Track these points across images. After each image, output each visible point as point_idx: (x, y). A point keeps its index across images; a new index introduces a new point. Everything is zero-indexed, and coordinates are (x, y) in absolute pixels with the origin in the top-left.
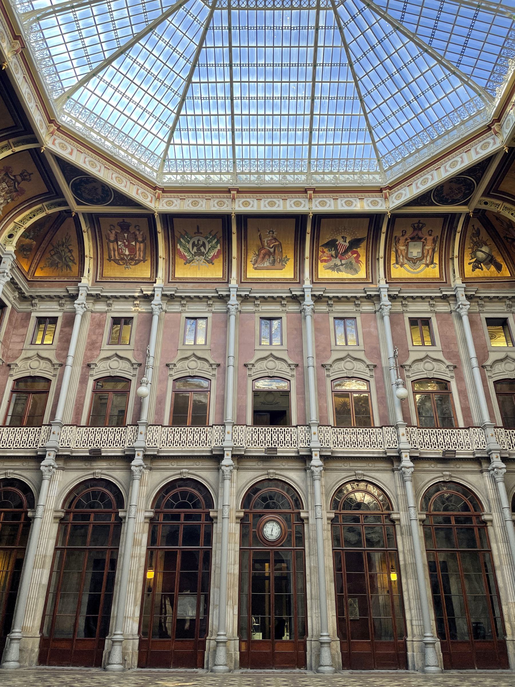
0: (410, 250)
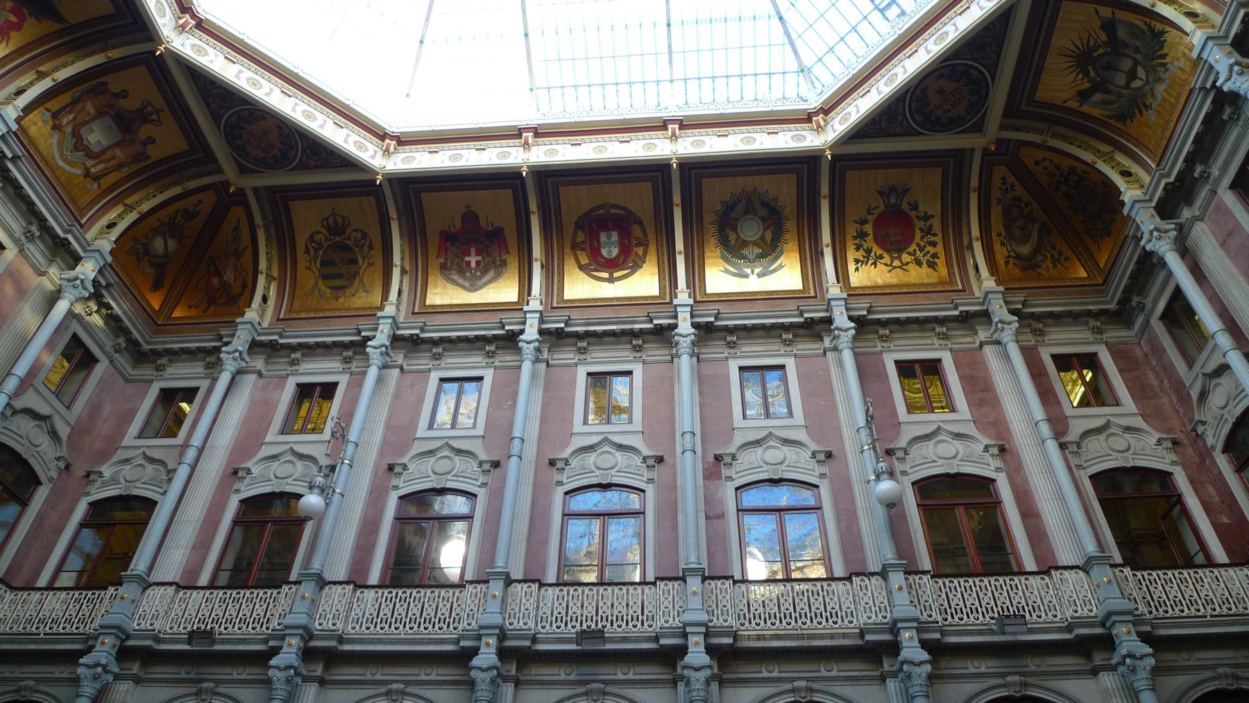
0: (94, 126)
